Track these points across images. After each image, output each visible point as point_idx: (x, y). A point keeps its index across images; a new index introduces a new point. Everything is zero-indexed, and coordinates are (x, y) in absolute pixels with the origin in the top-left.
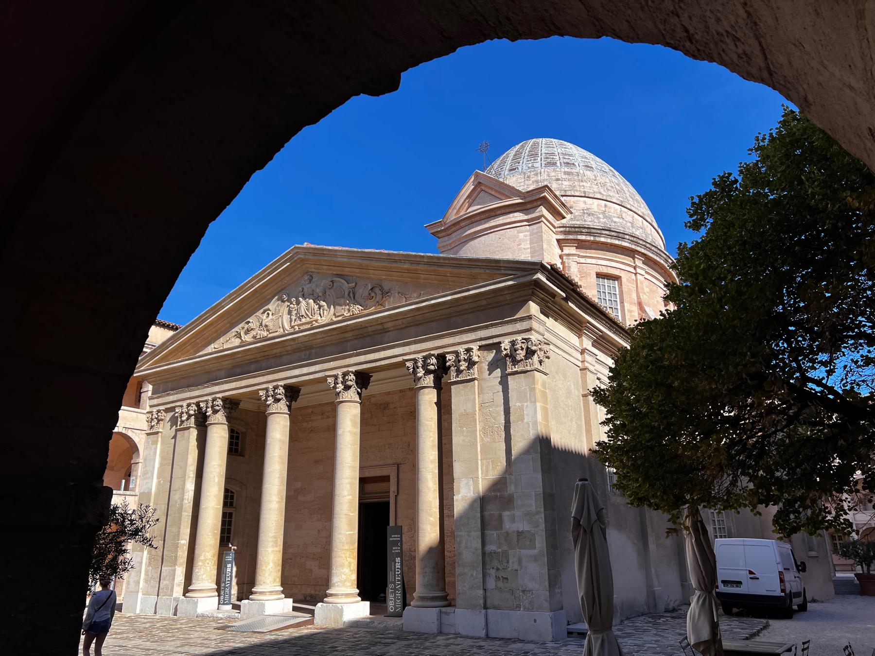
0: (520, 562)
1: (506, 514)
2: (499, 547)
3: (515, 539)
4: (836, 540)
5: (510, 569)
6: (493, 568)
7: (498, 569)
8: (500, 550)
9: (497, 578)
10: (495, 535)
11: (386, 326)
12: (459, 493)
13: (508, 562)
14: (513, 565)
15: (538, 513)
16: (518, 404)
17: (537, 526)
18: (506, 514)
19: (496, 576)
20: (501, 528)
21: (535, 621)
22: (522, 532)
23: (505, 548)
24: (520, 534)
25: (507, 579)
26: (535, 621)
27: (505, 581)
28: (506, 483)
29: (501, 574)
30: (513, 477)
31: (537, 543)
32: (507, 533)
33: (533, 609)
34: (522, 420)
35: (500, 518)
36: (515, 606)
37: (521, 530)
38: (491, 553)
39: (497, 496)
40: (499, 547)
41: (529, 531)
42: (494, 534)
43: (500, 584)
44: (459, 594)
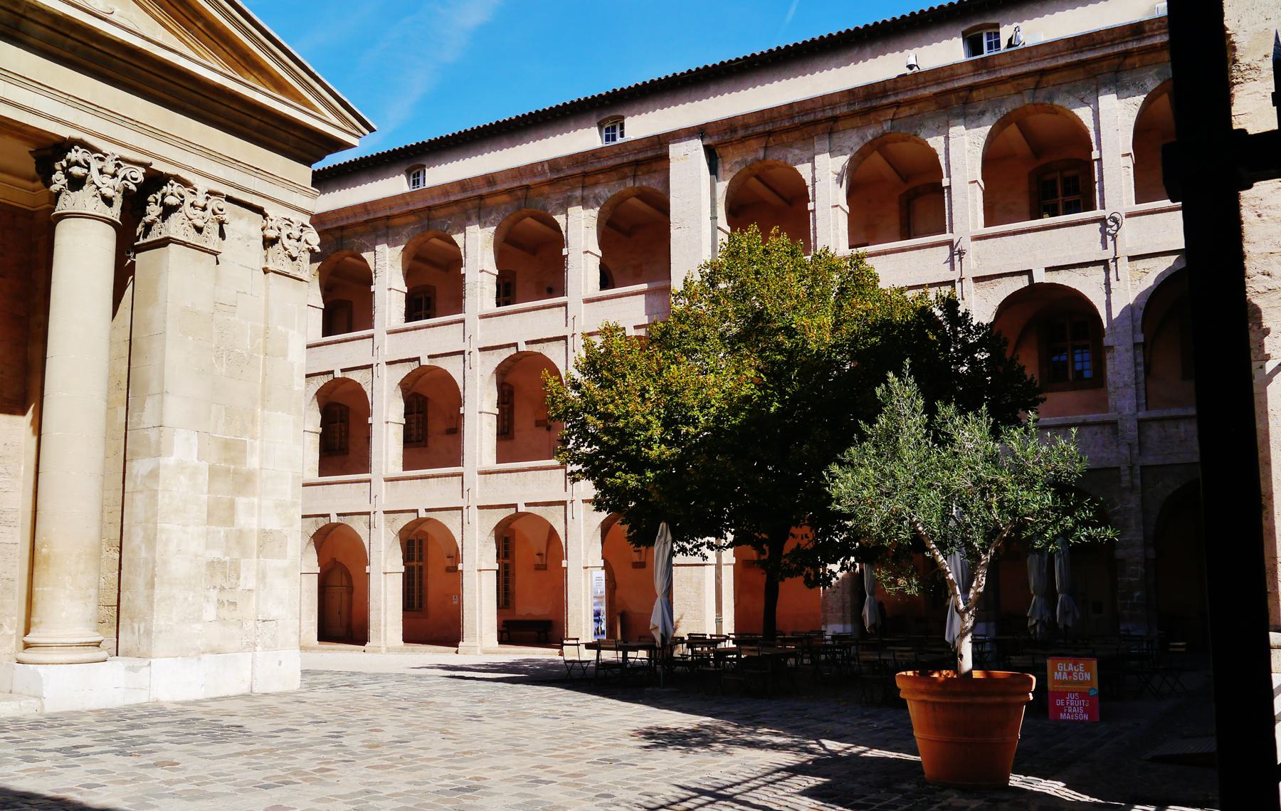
0: (262, 577)
1: (241, 501)
2: (226, 554)
3: (254, 543)
4: (413, 560)
5: (240, 589)
6: (215, 587)
7: (222, 589)
8: (227, 558)
9: (220, 603)
10: (222, 533)
11: (27, 25)
12: (171, 454)
13: (238, 578)
14: (248, 580)
15: (294, 504)
16: (280, 328)
17: (292, 525)
18: (241, 501)
19: (219, 600)
20: (233, 523)
21: (280, 663)
22: (271, 532)
23: (236, 555)
24: (265, 535)
25: (235, 604)
26: (280, 663)
27: (233, 607)
28: (244, 451)
29: (226, 597)
30: (257, 443)
31: (289, 549)
32: (241, 532)
33: (276, 646)
34: (285, 356)
35: (232, 506)
36: (244, 644)
37: (268, 528)
38: (213, 562)
39: (228, 471)
40: (226, 554)
41: (280, 532)
42: (219, 532)
43: (225, 613)
44: (160, 632)
